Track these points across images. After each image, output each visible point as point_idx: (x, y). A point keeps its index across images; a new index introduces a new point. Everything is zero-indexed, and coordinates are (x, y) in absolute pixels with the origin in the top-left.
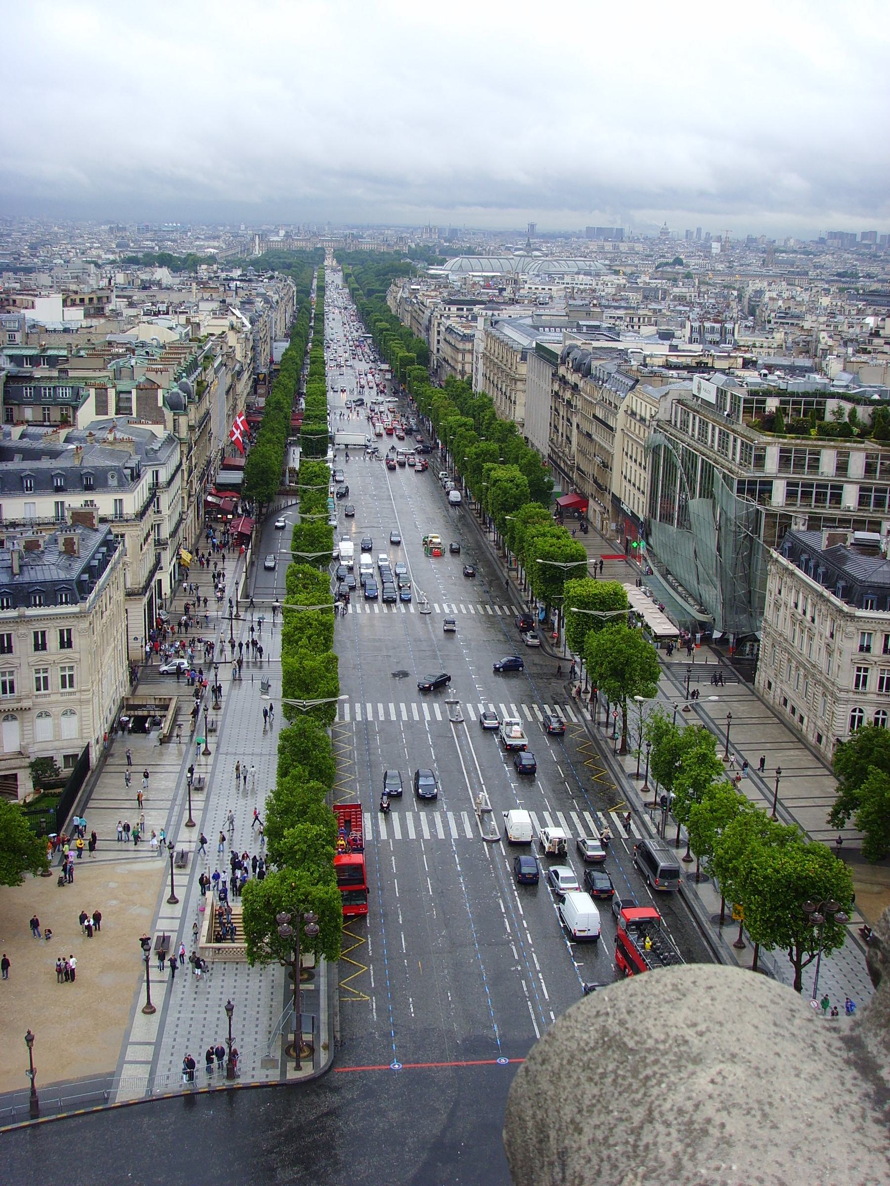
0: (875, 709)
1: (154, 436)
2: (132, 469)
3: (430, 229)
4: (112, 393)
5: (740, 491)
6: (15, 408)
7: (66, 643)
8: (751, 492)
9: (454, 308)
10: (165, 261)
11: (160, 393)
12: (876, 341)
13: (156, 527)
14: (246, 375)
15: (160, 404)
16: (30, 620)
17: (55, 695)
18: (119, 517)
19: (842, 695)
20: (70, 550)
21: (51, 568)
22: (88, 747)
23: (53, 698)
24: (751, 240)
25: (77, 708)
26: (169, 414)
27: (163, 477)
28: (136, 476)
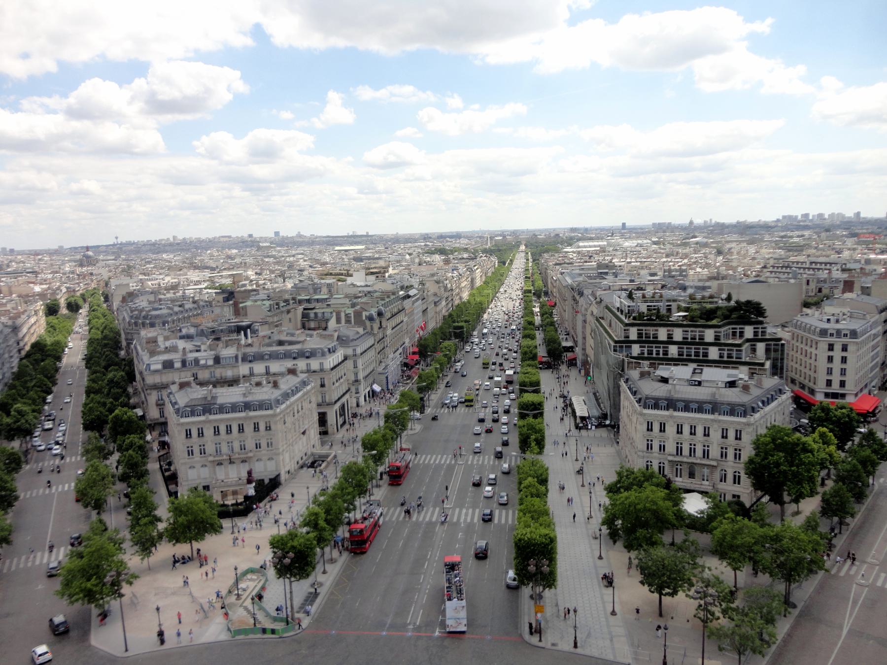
0: (658, 461)
1: (358, 333)
2: (329, 349)
3: (573, 230)
4: (343, 315)
5: (615, 351)
6: (307, 324)
7: (268, 428)
8: (621, 352)
9: (557, 267)
10: (442, 252)
11: (364, 314)
12: (765, 270)
13: (356, 374)
14: (444, 303)
15: (364, 318)
16: (251, 418)
17: (264, 451)
18: (322, 370)
19: (640, 453)
20: (276, 385)
21: (266, 393)
22: (279, 475)
23: (263, 452)
24: (738, 222)
25: (274, 457)
26: (368, 323)
27: (359, 351)
28: (332, 351)
